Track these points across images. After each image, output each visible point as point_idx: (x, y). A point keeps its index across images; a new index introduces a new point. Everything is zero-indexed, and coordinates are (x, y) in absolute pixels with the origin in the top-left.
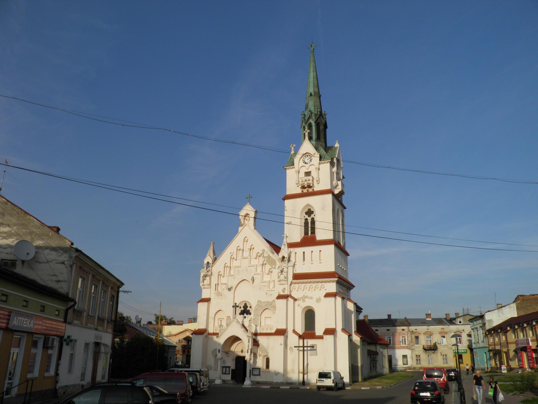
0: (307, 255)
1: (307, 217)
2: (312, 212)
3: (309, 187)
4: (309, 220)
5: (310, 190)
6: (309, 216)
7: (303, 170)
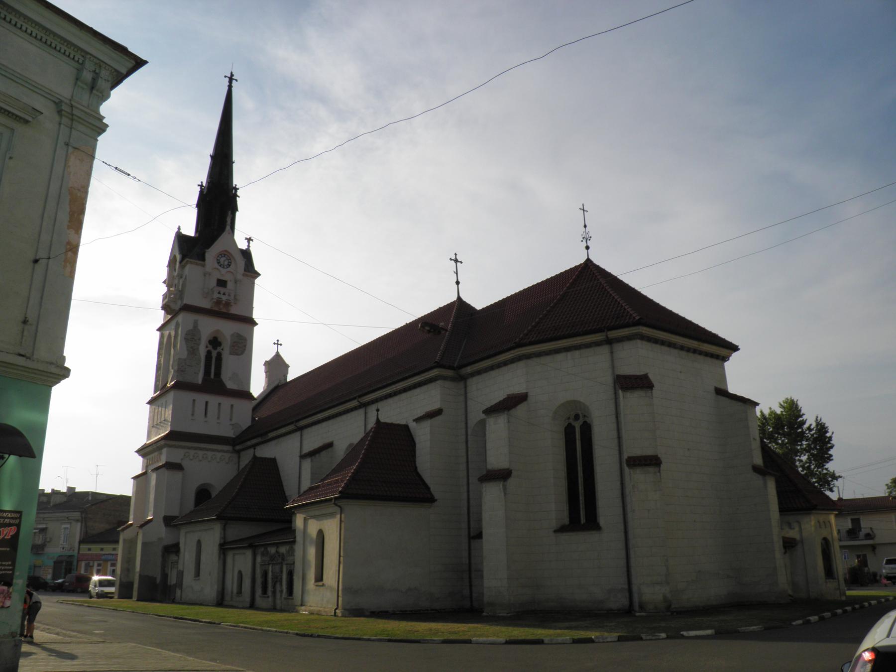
0: (212, 409)
1: (210, 348)
2: (220, 344)
3: (228, 304)
4: (214, 354)
5: (224, 310)
6: (215, 348)
7: (216, 275)
